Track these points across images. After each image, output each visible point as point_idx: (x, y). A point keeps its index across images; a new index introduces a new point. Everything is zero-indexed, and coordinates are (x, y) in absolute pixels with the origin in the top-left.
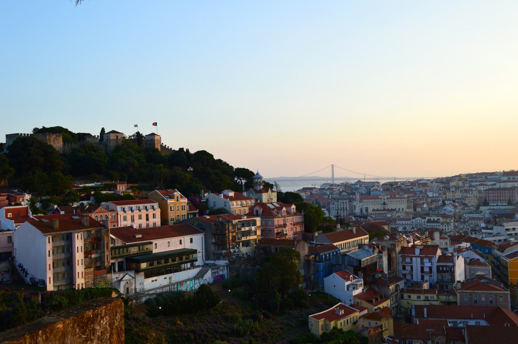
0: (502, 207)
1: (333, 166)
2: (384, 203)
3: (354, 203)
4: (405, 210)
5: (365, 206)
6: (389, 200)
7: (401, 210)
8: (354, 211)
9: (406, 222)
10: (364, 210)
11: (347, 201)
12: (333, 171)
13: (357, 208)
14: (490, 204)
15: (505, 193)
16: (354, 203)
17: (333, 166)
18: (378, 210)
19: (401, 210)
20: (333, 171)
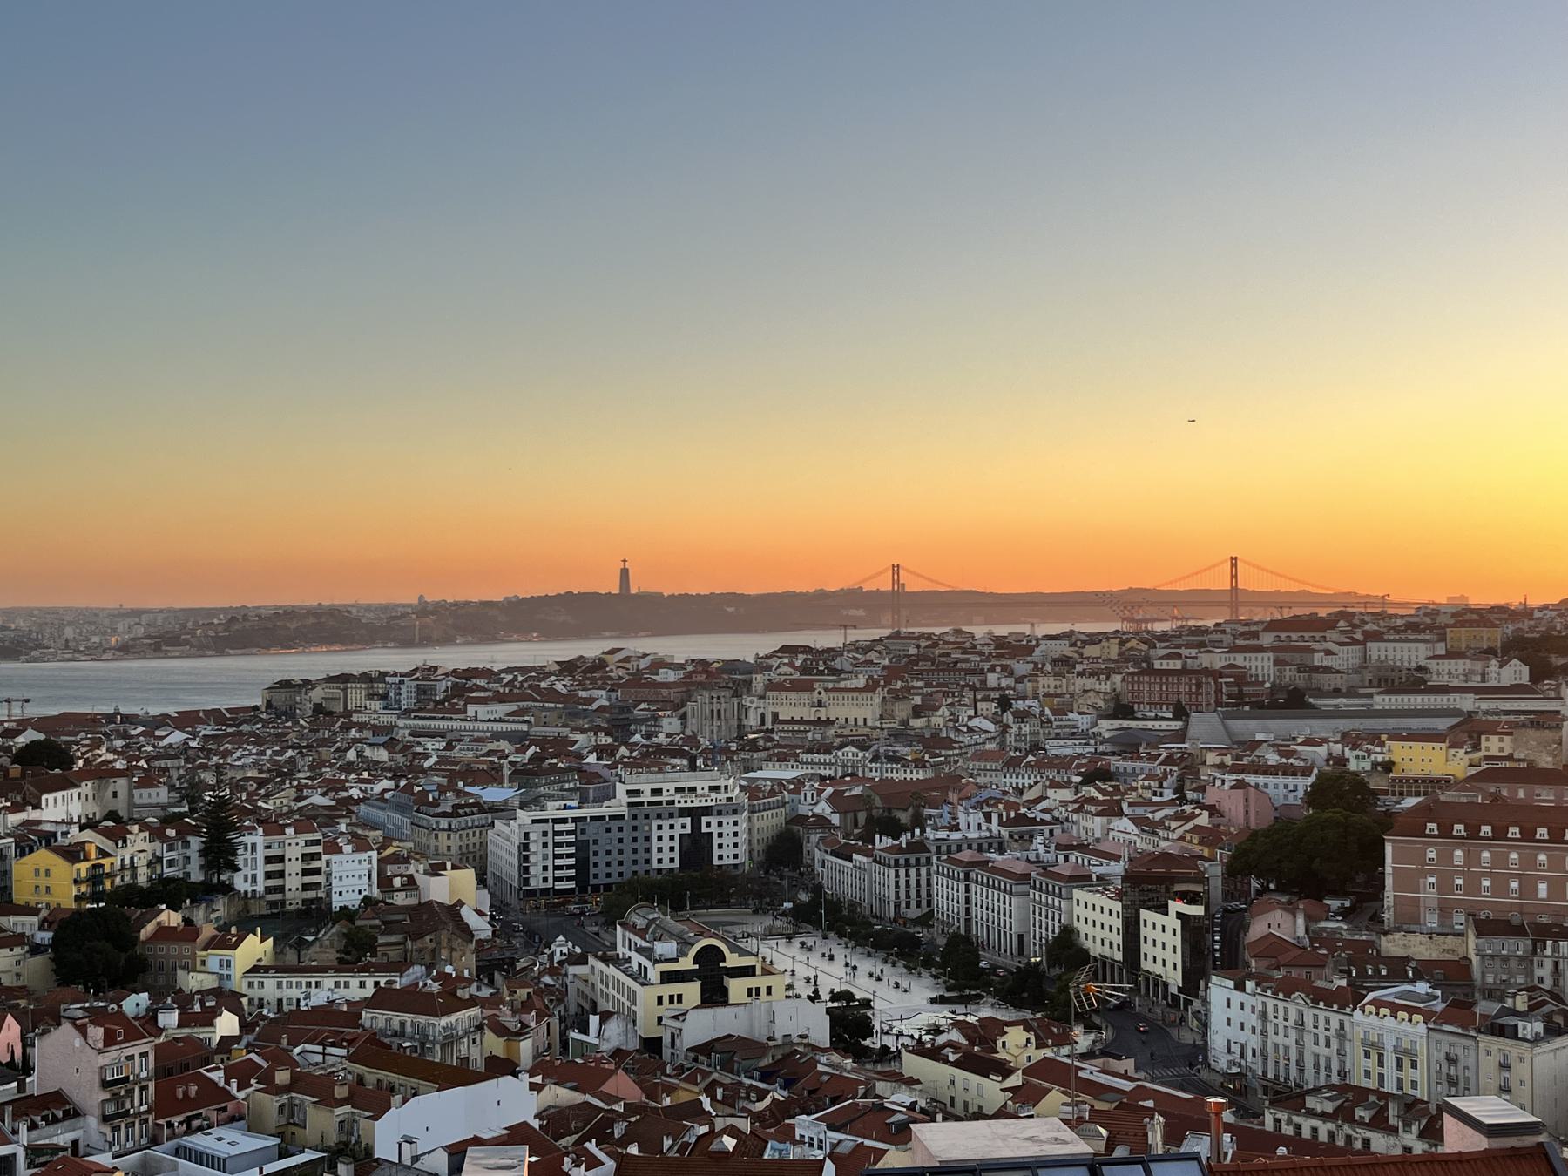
0: (1157, 724)
1: (1234, 561)
2: (820, 704)
3: (746, 701)
4: (869, 723)
5: (771, 709)
6: (831, 694)
7: (861, 722)
8: (745, 722)
9: (822, 757)
10: (769, 719)
11: (728, 693)
12: (1234, 576)
13: (751, 714)
14: (1139, 715)
15: (1179, 683)
16: (746, 701)
17: (1234, 561)
18: (802, 721)
19: (861, 722)
20: (1234, 576)
